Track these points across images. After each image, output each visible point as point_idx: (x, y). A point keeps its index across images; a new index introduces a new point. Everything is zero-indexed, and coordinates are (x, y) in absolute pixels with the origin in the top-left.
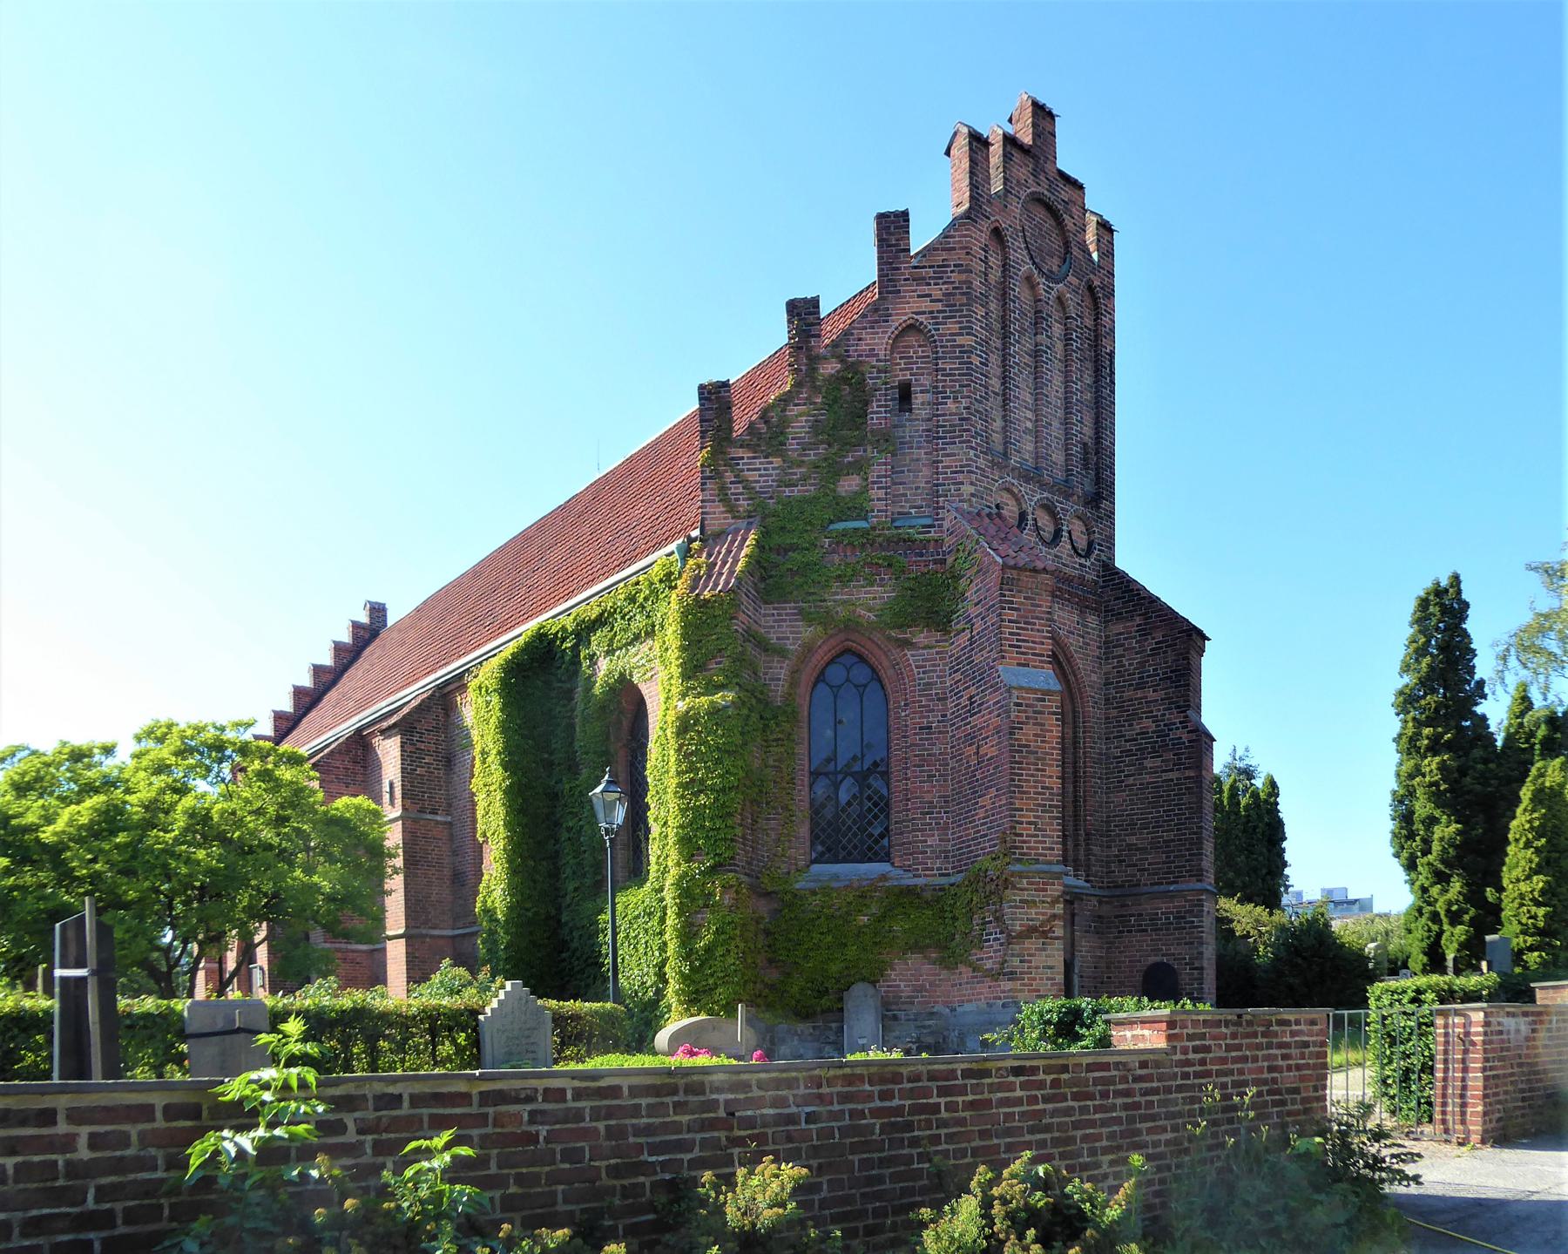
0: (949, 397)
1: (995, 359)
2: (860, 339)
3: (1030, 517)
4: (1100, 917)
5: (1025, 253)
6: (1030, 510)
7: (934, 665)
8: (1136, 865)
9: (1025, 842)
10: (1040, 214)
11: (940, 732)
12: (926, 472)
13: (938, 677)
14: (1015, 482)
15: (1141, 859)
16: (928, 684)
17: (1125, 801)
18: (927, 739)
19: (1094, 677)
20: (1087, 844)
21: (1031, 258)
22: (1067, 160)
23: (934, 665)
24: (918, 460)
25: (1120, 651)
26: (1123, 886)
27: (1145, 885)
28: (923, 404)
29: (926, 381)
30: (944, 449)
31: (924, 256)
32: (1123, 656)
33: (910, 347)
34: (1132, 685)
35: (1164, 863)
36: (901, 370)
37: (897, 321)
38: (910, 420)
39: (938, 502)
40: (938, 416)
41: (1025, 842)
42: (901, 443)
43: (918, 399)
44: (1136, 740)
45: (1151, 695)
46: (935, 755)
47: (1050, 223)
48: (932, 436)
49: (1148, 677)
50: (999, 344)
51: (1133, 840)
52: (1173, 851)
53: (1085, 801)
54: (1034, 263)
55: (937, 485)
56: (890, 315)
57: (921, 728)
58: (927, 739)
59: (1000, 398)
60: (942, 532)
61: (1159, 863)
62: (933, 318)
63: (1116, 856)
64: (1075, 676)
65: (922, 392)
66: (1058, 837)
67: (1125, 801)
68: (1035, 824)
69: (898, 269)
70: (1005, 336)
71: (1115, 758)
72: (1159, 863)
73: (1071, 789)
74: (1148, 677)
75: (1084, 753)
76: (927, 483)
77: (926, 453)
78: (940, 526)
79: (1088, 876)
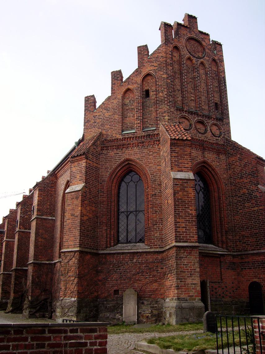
0: (160, 92)
1: (177, 82)
2: (133, 79)
3: (193, 125)
4: (233, 263)
5: (187, 52)
6: (193, 123)
7: (157, 174)
8: (245, 243)
9: (181, 235)
10: (193, 42)
11: (159, 196)
12: (154, 114)
13: (158, 177)
14: (187, 115)
15: (247, 240)
16: (155, 180)
17: (240, 219)
18: (155, 199)
19: (225, 176)
20: (226, 235)
21: (190, 53)
22: (201, 27)
23: (157, 174)
24: (151, 111)
25: (234, 166)
26: (242, 251)
27: (249, 250)
28: (153, 95)
29: (154, 88)
30: (159, 107)
31: (152, 55)
32: (235, 168)
33: (148, 80)
34: (238, 178)
35: (255, 242)
36: (146, 86)
37: (143, 74)
38: (149, 100)
39: (157, 123)
40: (157, 98)
41: (181, 235)
42: (146, 107)
43: (151, 94)
44: (241, 196)
45: (245, 180)
46: (157, 204)
47: (197, 44)
48: (156, 103)
49: (244, 174)
50: (179, 77)
51: (244, 233)
52: (258, 237)
53: (224, 219)
54: (191, 54)
55: (157, 118)
56: (142, 72)
57: (153, 195)
58: (155, 199)
59: (180, 91)
60: (159, 131)
61: (253, 242)
62: (155, 71)
63: (238, 239)
64: (217, 176)
65: (152, 92)
66: (196, 232)
67: (240, 219)
68: (185, 227)
69: (144, 60)
70: (181, 74)
71: (235, 203)
72: (253, 242)
73: (219, 215)
74: (244, 174)
75: (223, 202)
76: (154, 117)
77: (154, 109)
78: (158, 130)
79: (227, 247)
